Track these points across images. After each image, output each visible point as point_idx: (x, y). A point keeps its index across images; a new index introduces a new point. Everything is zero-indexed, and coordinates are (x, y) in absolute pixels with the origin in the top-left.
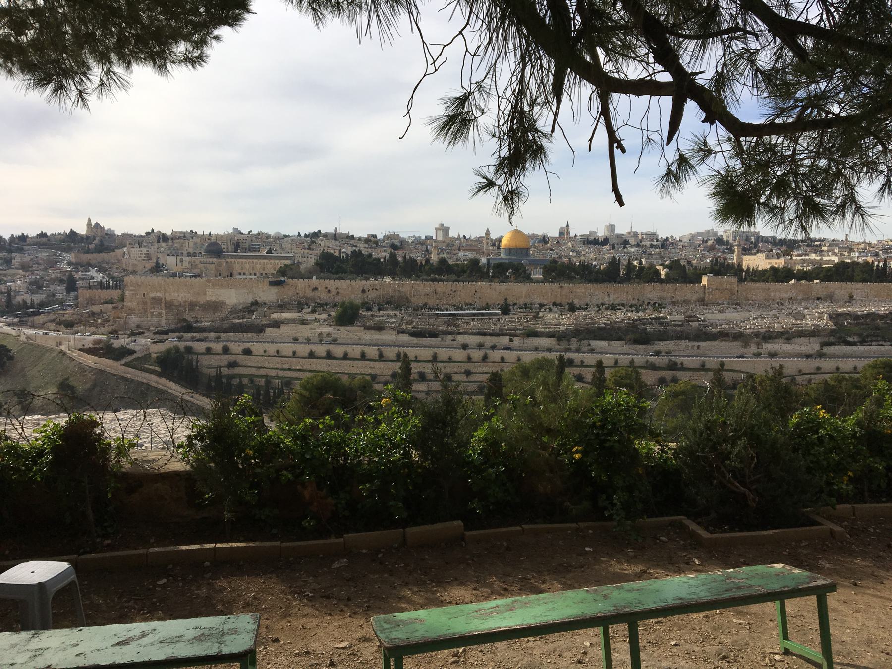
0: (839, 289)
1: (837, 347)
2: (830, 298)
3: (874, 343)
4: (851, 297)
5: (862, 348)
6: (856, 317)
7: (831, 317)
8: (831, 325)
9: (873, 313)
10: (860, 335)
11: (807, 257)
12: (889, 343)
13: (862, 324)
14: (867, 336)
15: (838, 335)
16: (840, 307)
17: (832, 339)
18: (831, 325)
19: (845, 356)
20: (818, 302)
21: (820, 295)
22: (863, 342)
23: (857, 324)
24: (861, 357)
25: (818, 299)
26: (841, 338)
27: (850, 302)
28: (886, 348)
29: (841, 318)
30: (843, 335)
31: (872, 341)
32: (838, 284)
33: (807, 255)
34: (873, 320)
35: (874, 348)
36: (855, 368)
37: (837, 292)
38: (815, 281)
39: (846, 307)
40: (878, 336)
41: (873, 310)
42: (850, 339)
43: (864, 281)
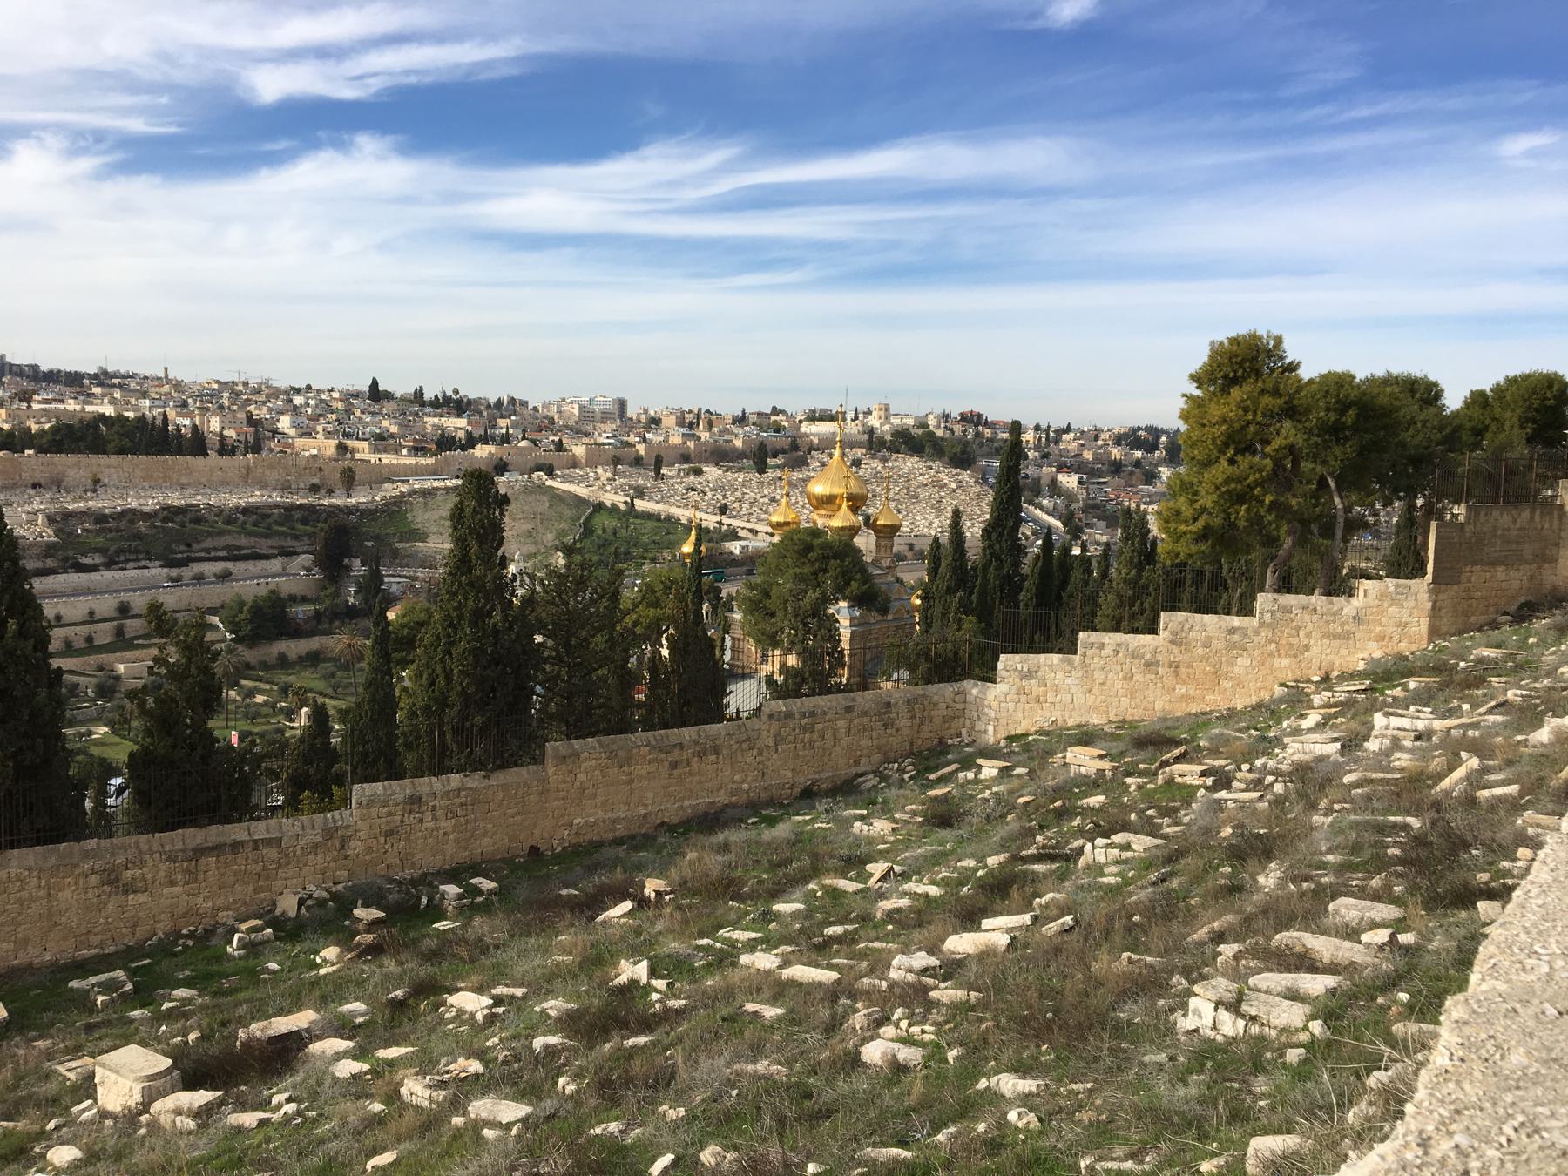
0: (74, 466)
1: (61, 578)
2: (57, 483)
3: (132, 564)
4: (97, 481)
5: (108, 575)
6: (100, 518)
7: (51, 520)
8: (49, 535)
9: (133, 511)
10: (103, 551)
11: (61, 406)
12: (157, 563)
13: (110, 530)
14: (120, 551)
15: (60, 554)
16: (74, 500)
17: (50, 563)
18: (49, 535)
19: (77, 592)
20: (32, 492)
21: (39, 477)
22: (110, 564)
23: (98, 533)
24: (106, 592)
25: (34, 486)
26: (66, 559)
27: (94, 491)
28: (154, 571)
29: (73, 522)
30: (71, 553)
31: (128, 561)
32: (71, 459)
33: (62, 401)
34: (132, 522)
35: (131, 573)
36: (91, 613)
37: (71, 472)
38: (27, 452)
39: (86, 500)
40: (137, 551)
41: (134, 504)
42: (86, 561)
43: (121, 451)
